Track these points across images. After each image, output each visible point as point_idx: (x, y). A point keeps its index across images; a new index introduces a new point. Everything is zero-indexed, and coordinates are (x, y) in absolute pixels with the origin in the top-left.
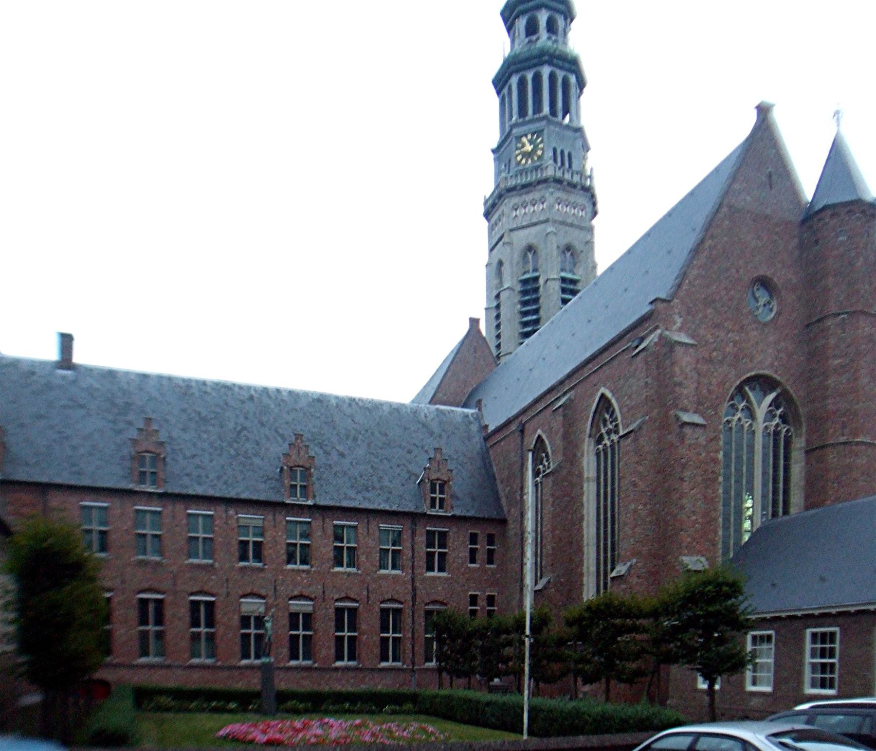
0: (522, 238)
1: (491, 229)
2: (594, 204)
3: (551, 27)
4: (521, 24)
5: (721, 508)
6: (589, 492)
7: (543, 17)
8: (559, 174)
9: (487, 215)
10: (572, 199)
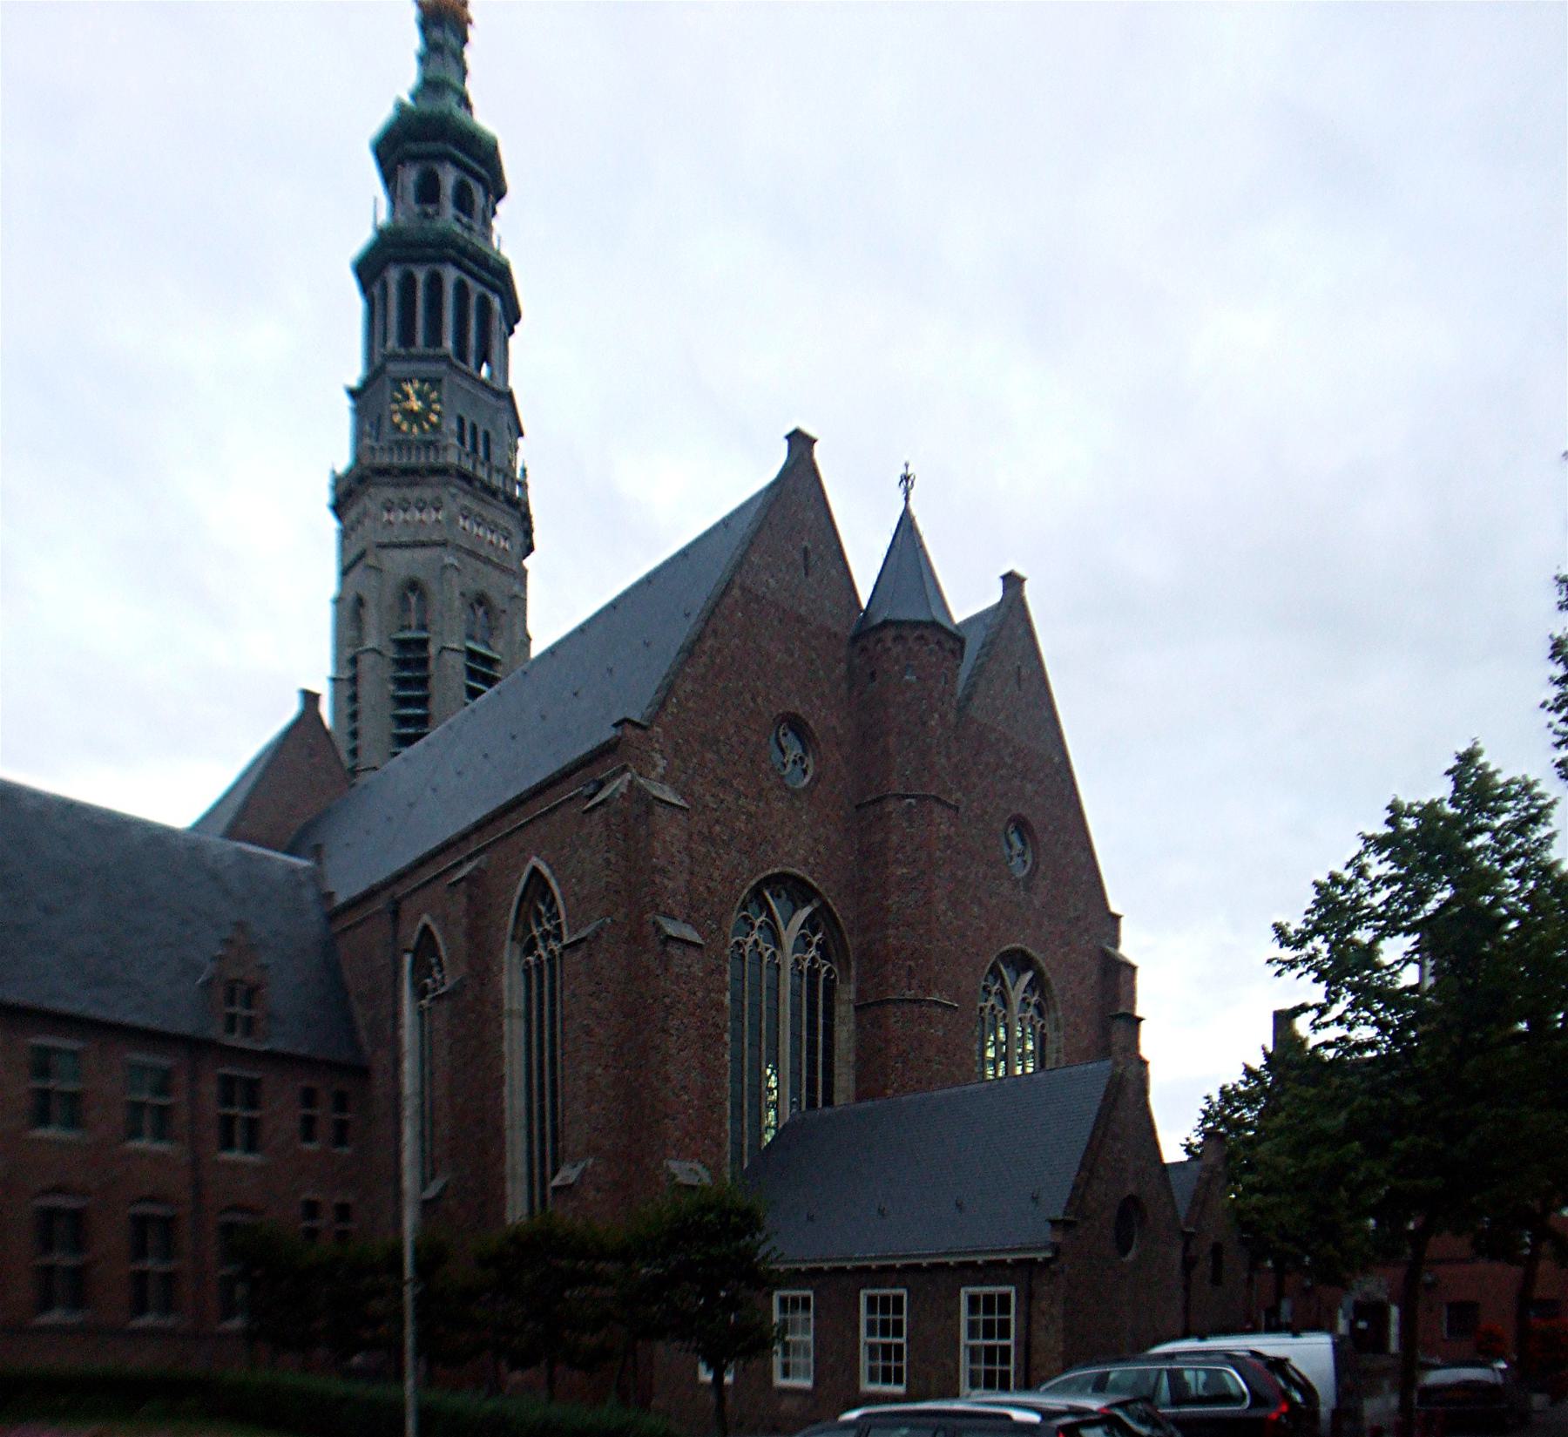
0: (400, 564)
1: (345, 535)
2: (528, 532)
3: (463, 201)
4: (410, 176)
5: (728, 1085)
6: (513, 1034)
7: (449, 178)
8: (468, 465)
9: (338, 508)
10: (489, 514)
